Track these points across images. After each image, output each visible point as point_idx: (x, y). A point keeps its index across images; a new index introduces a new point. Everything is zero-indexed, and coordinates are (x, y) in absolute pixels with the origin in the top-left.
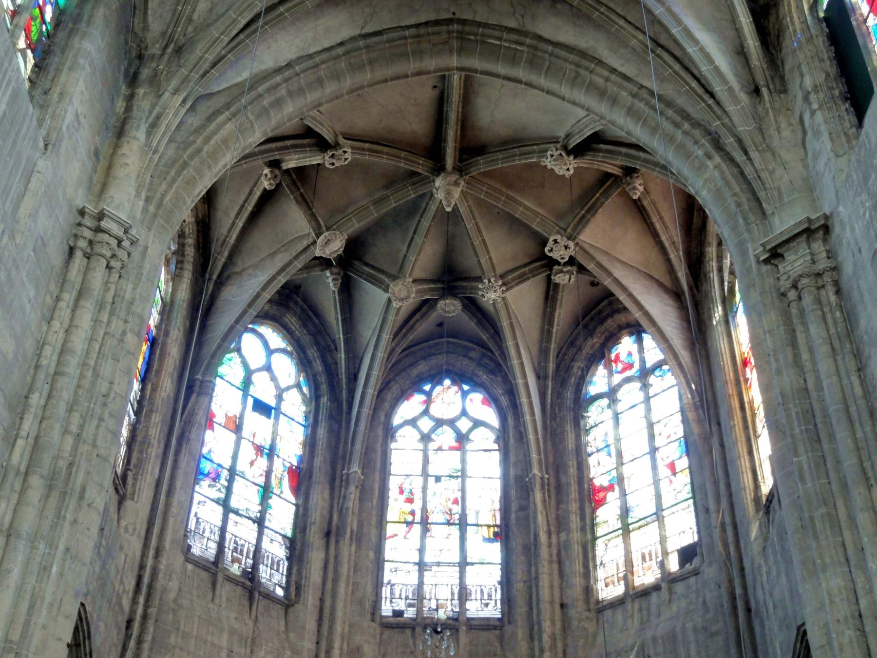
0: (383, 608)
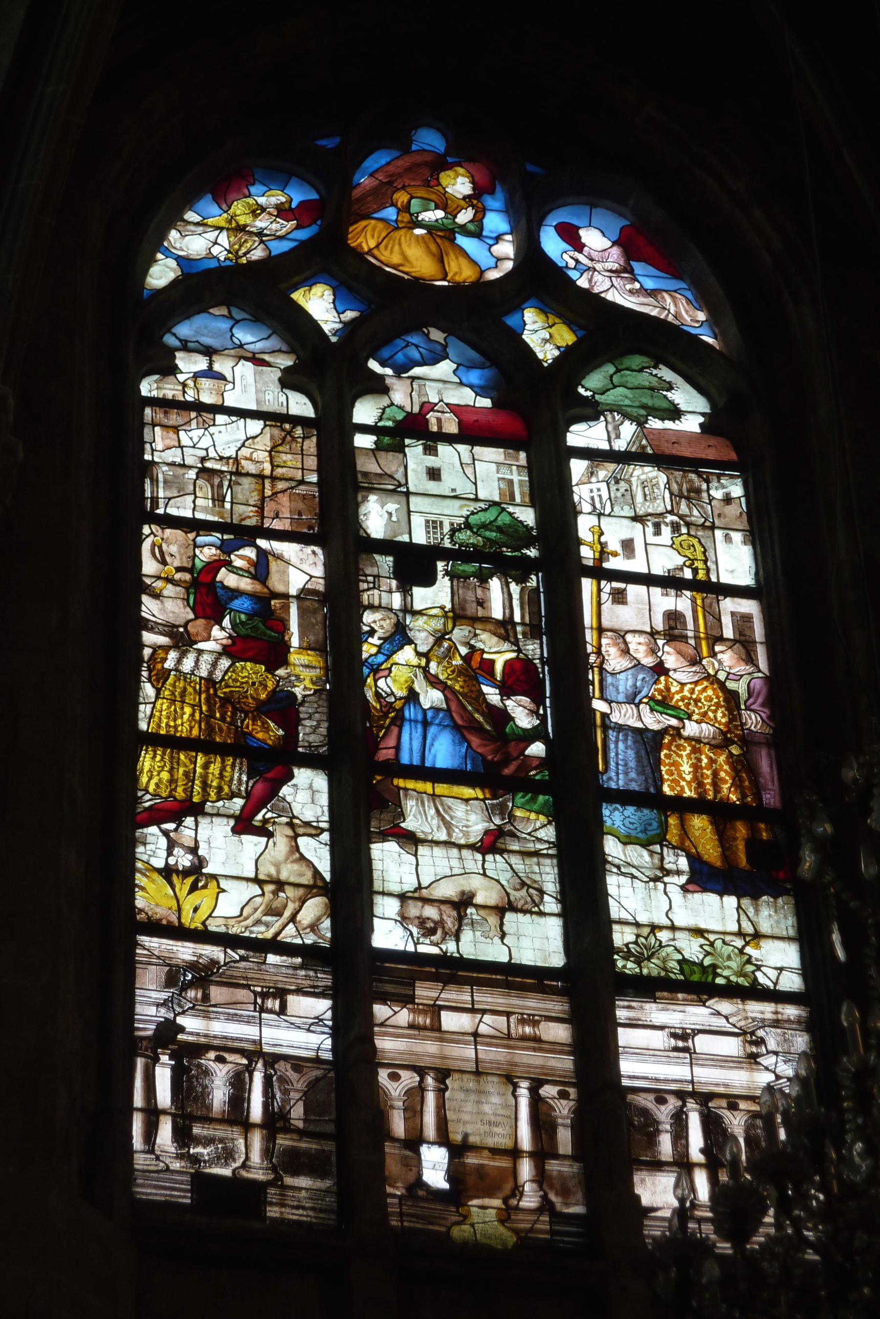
0: (141, 1161)
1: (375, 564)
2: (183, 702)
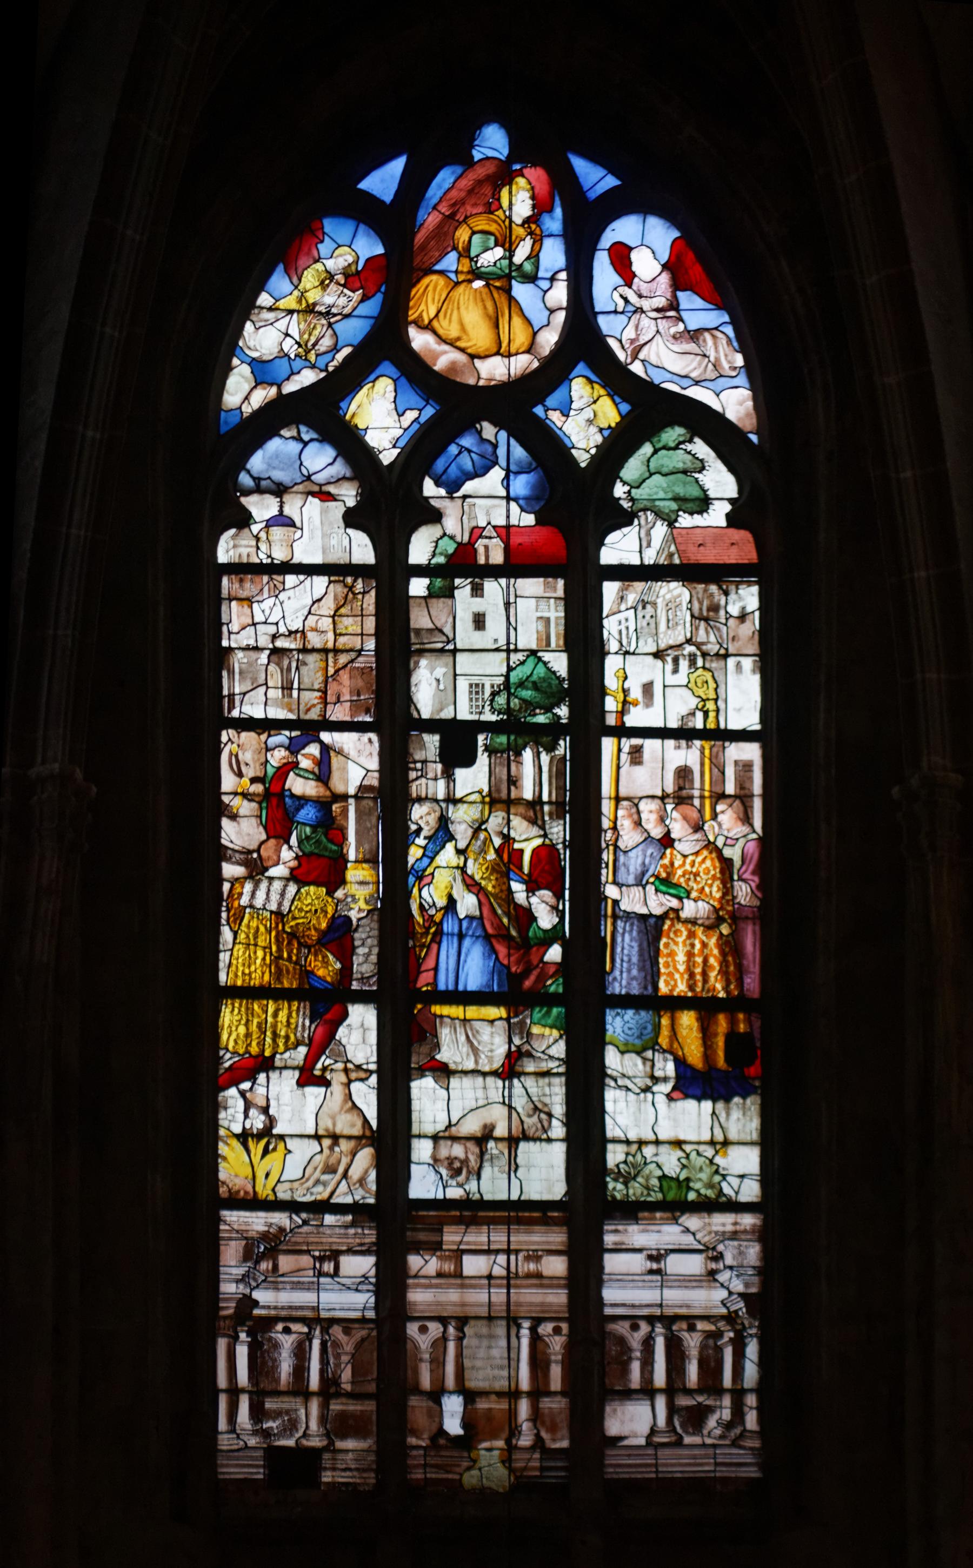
0: (225, 1442)
1: (423, 746)
2: (256, 945)
